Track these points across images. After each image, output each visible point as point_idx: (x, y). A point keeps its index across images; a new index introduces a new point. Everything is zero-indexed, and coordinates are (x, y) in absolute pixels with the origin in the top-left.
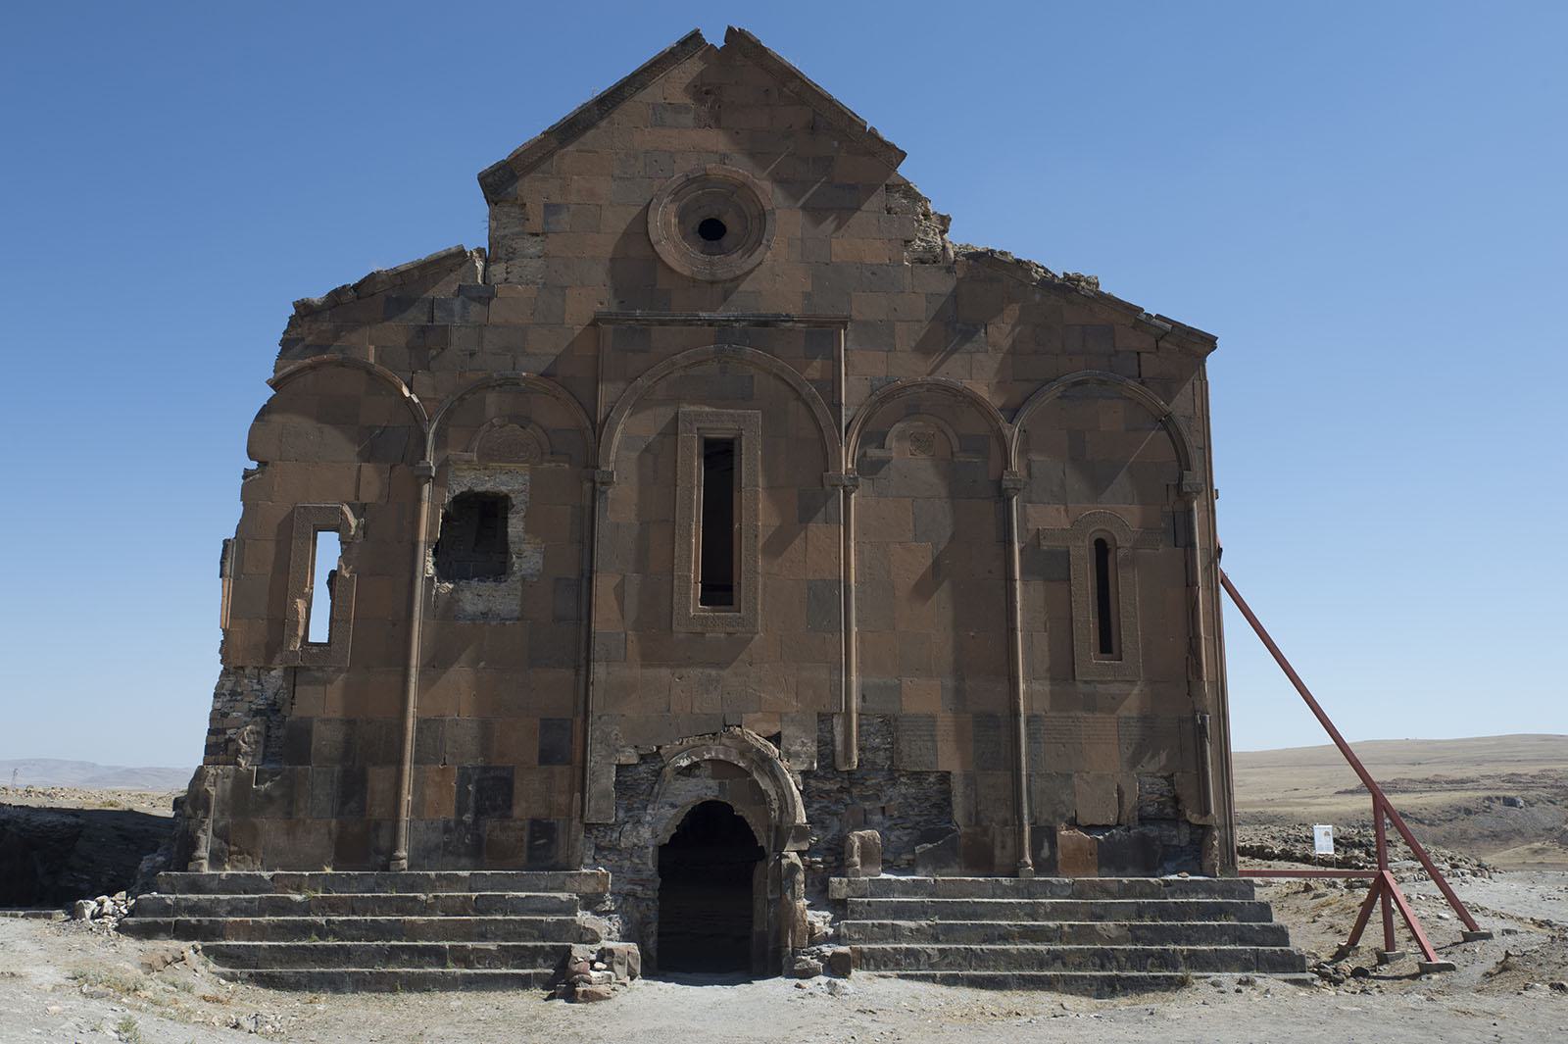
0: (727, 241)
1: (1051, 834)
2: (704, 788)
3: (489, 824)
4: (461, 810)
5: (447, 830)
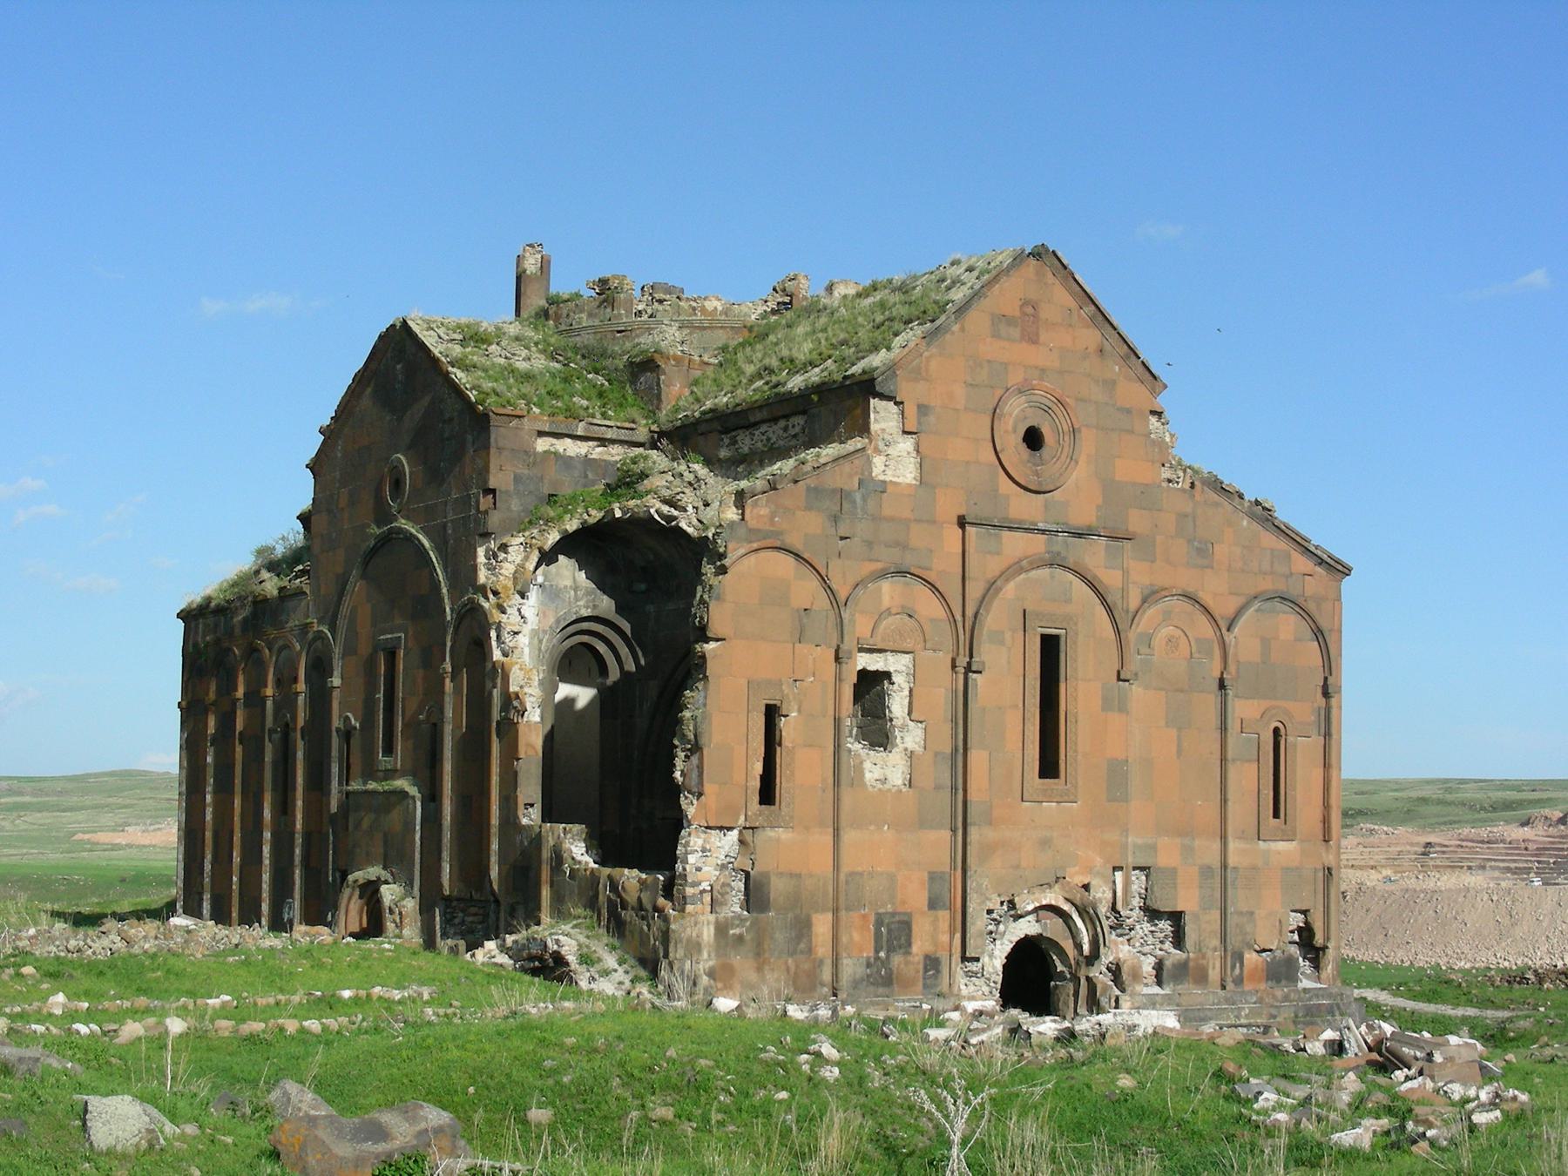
0: (1046, 451)
1: (1239, 957)
2: (1027, 927)
3: (897, 960)
4: (877, 952)
5: (868, 965)
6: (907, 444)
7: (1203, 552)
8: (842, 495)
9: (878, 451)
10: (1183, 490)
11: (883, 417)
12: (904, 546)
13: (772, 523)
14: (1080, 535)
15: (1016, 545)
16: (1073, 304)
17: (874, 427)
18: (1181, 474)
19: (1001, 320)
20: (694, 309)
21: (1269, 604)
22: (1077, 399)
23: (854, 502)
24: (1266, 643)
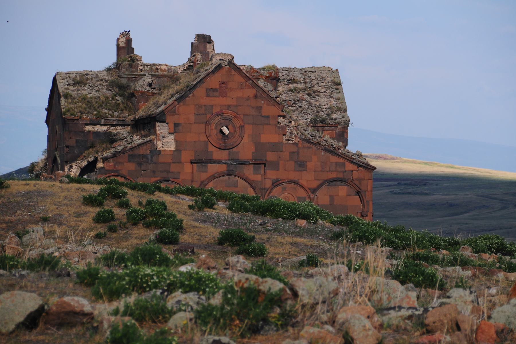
6: (172, 137)
7: (302, 166)
8: (145, 156)
9: (160, 140)
10: (293, 144)
11: (162, 129)
12: (168, 172)
13: (115, 167)
14: (242, 164)
15: (213, 169)
16: (242, 80)
17: (158, 132)
18: (293, 137)
19: (210, 92)
20: (157, 69)
21: (333, 183)
22: (244, 115)
23: (148, 158)
24: (332, 198)
